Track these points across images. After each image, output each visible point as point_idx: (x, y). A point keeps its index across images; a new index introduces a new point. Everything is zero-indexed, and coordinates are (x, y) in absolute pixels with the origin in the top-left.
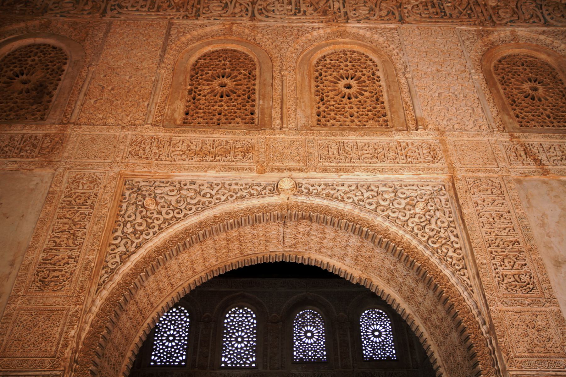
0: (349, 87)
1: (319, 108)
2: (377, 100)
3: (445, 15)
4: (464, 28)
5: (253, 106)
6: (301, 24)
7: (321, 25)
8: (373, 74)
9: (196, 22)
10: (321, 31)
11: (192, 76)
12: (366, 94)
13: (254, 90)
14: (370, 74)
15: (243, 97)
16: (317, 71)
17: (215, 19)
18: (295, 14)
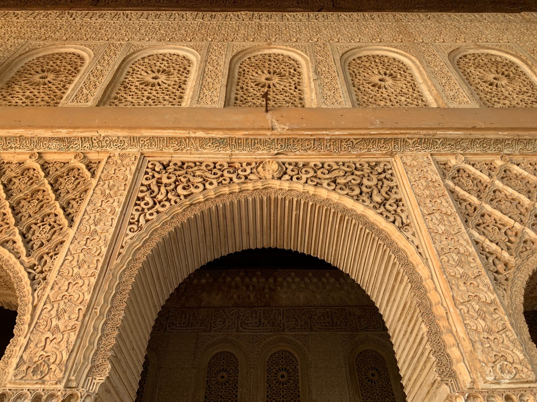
0: (283, 376)
1: (268, 392)
2: (296, 385)
3: (334, 324)
4: (342, 333)
5: (237, 392)
6: (260, 333)
7: (271, 333)
8: (295, 367)
9: (210, 333)
10: (271, 338)
11: (208, 371)
12: (291, 381)
13: (237, 380)
14: (294, 367)
15: (232, 385)
16: (268, 366)
17: (219, 332)
18: (258, 326)
